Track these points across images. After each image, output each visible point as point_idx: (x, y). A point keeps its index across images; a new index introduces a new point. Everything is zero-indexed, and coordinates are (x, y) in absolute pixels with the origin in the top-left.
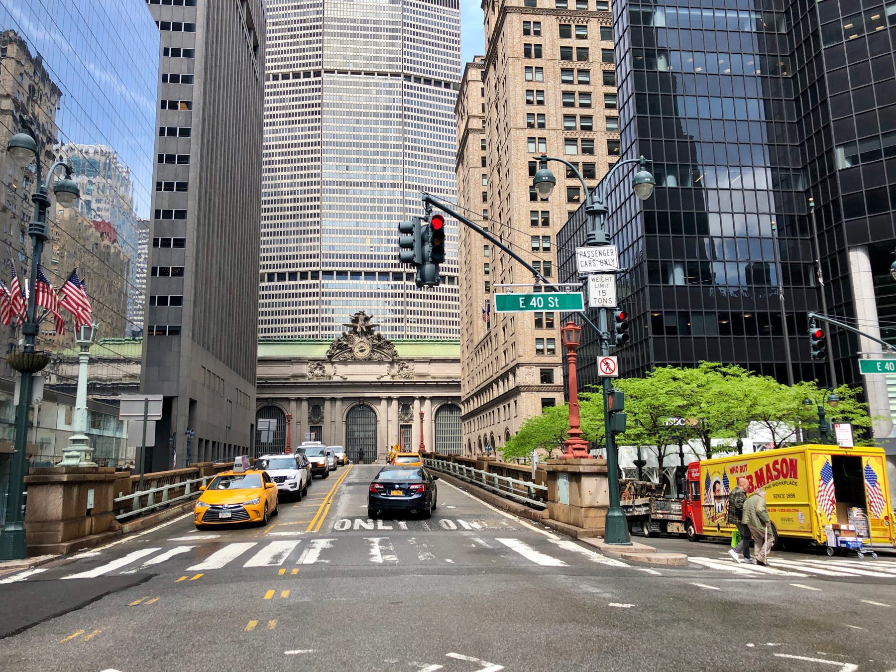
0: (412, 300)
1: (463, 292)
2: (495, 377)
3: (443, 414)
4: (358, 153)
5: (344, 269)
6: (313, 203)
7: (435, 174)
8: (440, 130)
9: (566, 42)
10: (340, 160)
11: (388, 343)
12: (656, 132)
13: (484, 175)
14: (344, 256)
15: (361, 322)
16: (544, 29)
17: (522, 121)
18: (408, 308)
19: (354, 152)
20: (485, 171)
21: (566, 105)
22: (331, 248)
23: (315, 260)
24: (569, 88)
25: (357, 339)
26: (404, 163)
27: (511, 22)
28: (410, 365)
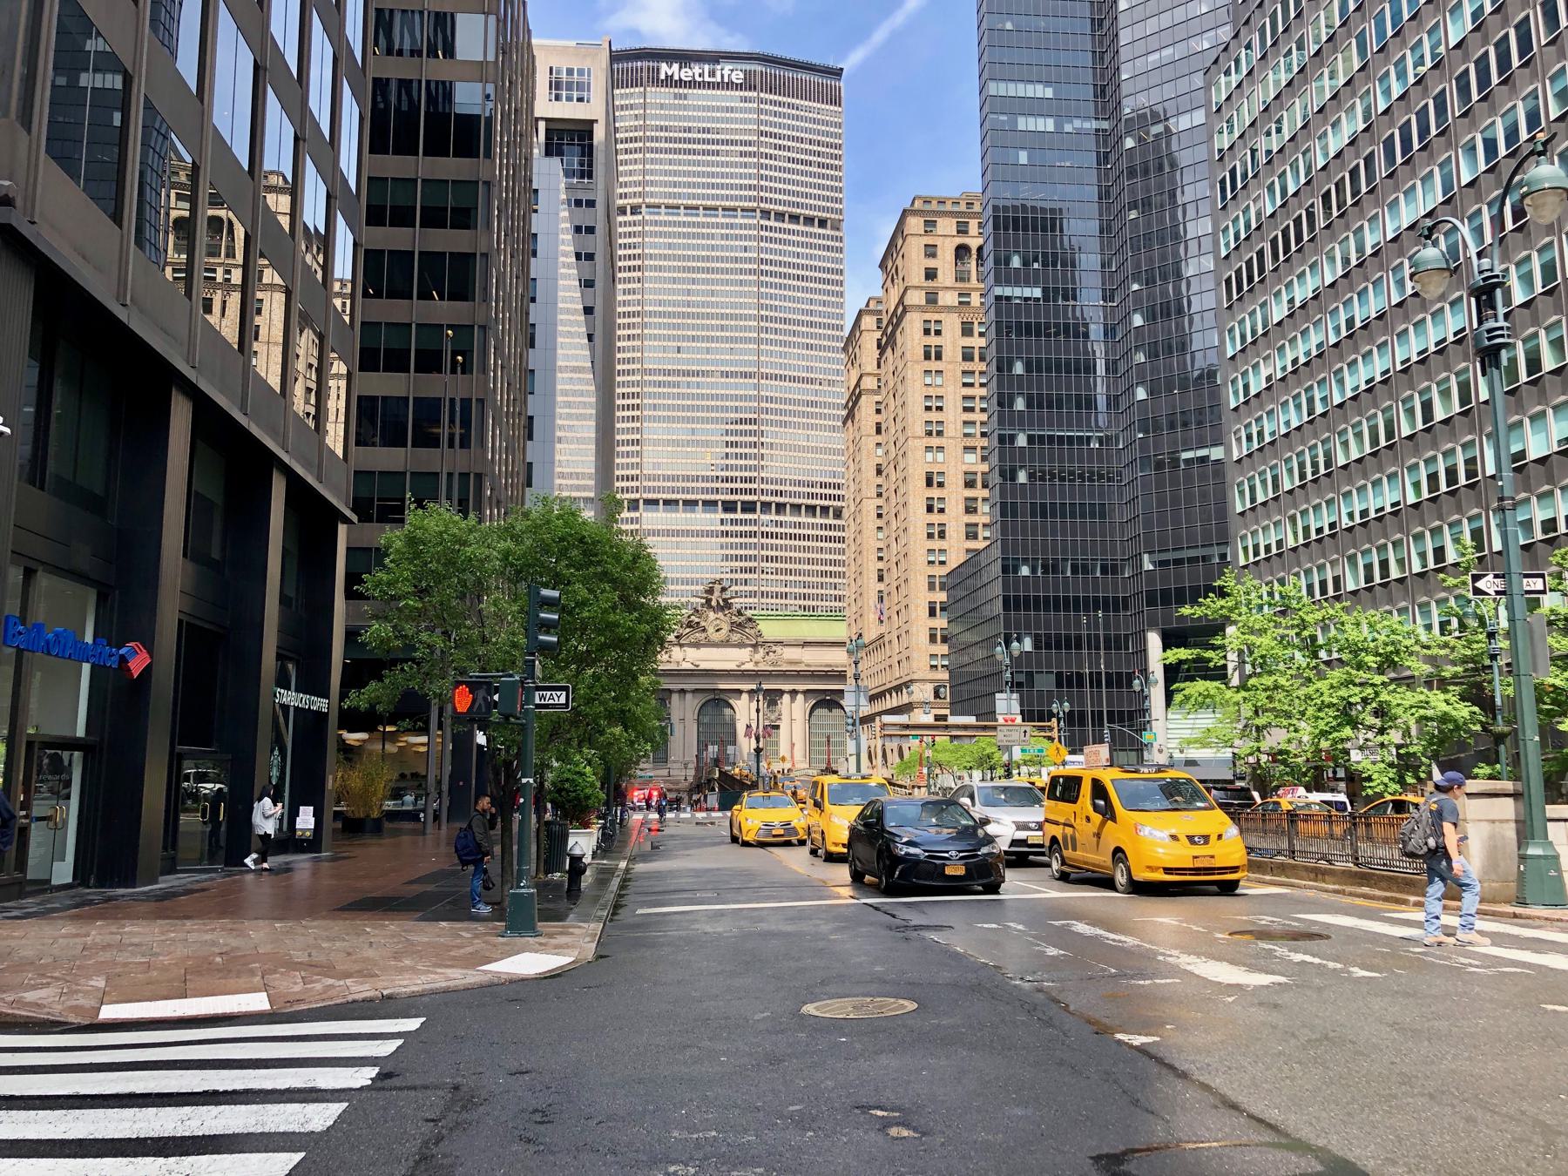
0: (769, 541)
1: (850, 554)
2: (888, 686)
3: (818, 712)
4: (694, 327)
5: (674, 496)
6: (630, 402)
7: (803, 357)
8: (811, 291)
9: (968, 341)
10: (669, 338)
11: (750, 620)
12: (1015, 533)
13: (878, 444)
14: (674, 478)
15: (717, 593)
16: (945, 328)
17: (920, 429)
18: (764, 553)
19: (689, 327)
20: (879, 439)
21: (966, 409)
22: (657, 465)
23: (634, 484)
24: (969, 391)
25: (712, 615)
26: (759, 341)
27: (911, 321)
28: (778, 649)
